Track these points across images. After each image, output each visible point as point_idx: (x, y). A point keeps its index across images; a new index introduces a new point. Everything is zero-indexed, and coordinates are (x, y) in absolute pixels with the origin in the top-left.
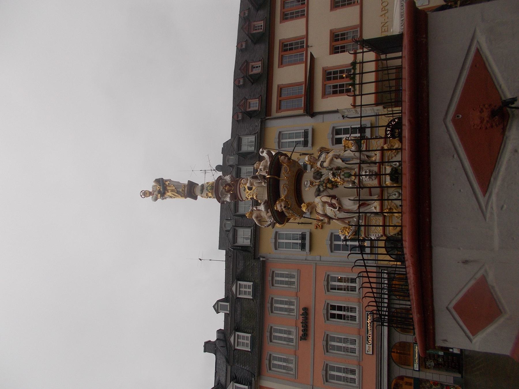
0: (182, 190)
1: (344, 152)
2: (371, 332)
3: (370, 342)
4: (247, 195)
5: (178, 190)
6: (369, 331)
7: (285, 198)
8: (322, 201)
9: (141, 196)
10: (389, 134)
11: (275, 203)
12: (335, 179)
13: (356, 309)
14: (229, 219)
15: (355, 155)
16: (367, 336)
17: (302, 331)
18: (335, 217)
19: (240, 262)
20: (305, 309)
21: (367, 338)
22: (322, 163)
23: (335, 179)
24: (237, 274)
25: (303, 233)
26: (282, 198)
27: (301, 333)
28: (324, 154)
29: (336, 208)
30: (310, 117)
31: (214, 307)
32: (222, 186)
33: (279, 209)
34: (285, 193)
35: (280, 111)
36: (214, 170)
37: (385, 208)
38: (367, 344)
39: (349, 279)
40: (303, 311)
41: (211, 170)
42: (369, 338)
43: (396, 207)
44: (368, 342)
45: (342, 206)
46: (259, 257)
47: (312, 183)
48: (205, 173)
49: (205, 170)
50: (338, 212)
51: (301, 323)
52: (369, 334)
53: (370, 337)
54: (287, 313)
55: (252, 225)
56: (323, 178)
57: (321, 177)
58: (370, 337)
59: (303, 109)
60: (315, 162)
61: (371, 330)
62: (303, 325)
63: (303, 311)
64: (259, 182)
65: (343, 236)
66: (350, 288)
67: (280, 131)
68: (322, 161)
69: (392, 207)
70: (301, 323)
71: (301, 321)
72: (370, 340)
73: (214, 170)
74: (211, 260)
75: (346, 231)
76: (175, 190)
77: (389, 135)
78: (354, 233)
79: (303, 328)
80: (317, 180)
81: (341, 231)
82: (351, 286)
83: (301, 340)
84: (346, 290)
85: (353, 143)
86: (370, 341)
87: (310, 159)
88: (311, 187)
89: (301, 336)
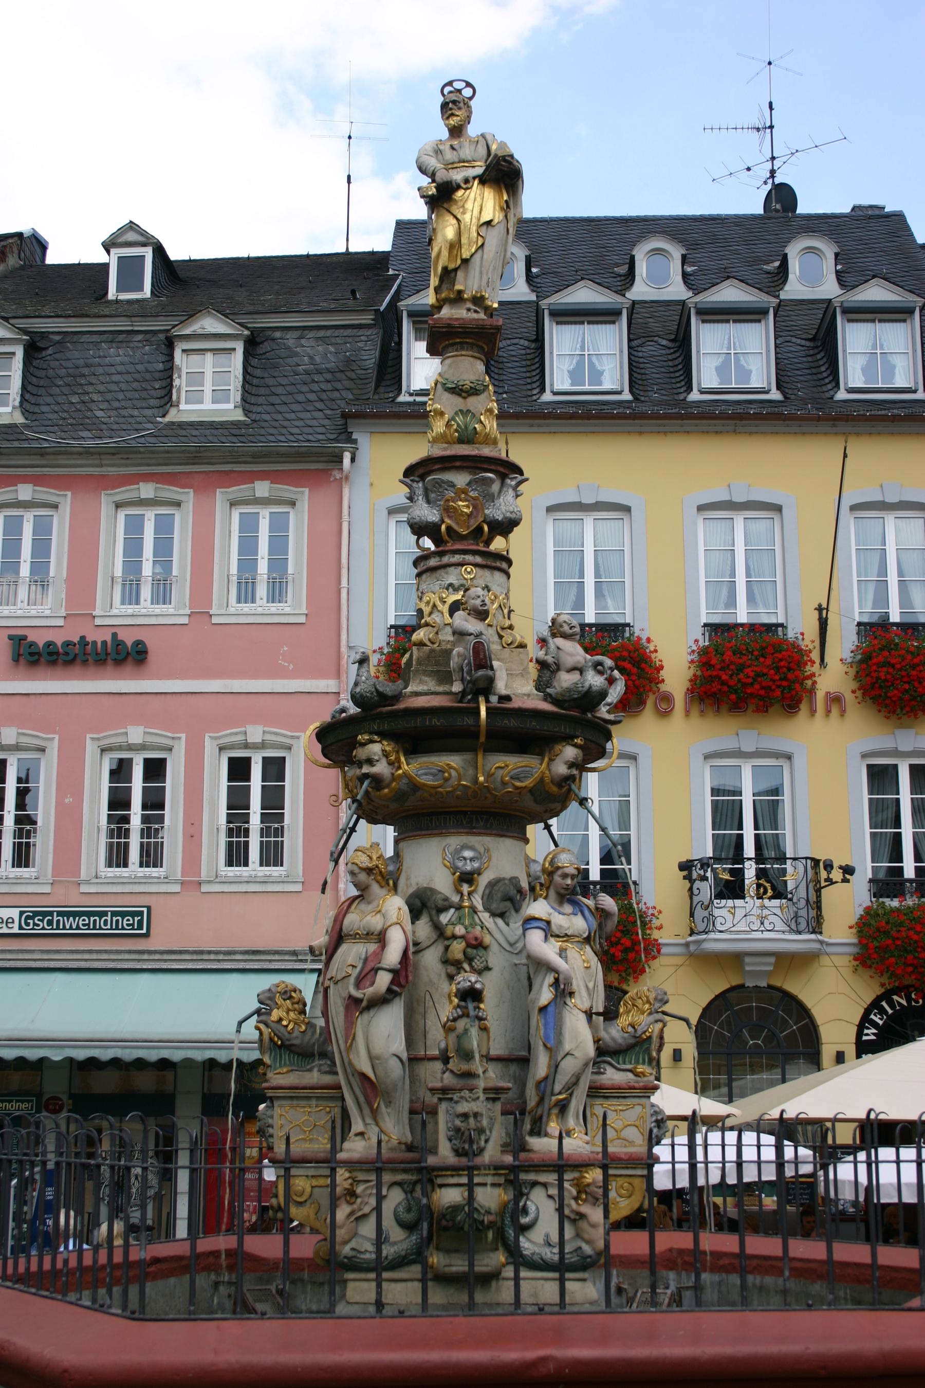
0: (460, 292)
1: (585, 1012)
2: (68, 927)
3: (28, 924)
4: (435, 599)
6: (71, 919)
7: (405, 774)
8: (387, 929)
9: (450, 83)
10: (909, 999)
11: (383, 735)
13: (155, 866)
14: (534, 270)
15: (567, 1054)
16: (51, 914)
17: (49, 644)
18: (330, 979)
19: (332, 349)
20: (139, 653)
21: (44, 914)
24: (278, 334)
27: (40, 639)
28: (586, 926)
31: (132, 226)
32: (469, 484)
36: (773, 173)
37: (355, 1174)
38: (21, 913)
39: (276, 836)
40: (129, 643)
41: (773, 158)
42: (42, 921)
43: (360, 1214)
44: (28, 918)
46: (354, 437)
47: (468, 878)
48: (758, 129)
49: (771, 127)
51: (83, 638)
52: (58, 921)
53: (50, 923)
54: (120, 574)
56: (491, 920)
57: (493, 915)
58: (50, 923)
60: (552, 888)
61: (74, 927)
62: (75, 645)
63: (129, 643)
66: (238, 843)
68: (548, 923)
69: (359, 1200)
70: (83, 638)
71: (89, 639)
72: (38, 925)
73: (773, 173)
74: (349, 181)
75: (288, 1011)
76: (459, 262)
77: (904, 1002)
79: (59, 644)
80: (482, 899)
81: (286, 992)
82: (246, 844)
83: (11, 638)
84: (231, 825)
85: (636, 1030)
86: (31, 927)
87: (559, 872)
88: (454, 874)
89: (29, 639)
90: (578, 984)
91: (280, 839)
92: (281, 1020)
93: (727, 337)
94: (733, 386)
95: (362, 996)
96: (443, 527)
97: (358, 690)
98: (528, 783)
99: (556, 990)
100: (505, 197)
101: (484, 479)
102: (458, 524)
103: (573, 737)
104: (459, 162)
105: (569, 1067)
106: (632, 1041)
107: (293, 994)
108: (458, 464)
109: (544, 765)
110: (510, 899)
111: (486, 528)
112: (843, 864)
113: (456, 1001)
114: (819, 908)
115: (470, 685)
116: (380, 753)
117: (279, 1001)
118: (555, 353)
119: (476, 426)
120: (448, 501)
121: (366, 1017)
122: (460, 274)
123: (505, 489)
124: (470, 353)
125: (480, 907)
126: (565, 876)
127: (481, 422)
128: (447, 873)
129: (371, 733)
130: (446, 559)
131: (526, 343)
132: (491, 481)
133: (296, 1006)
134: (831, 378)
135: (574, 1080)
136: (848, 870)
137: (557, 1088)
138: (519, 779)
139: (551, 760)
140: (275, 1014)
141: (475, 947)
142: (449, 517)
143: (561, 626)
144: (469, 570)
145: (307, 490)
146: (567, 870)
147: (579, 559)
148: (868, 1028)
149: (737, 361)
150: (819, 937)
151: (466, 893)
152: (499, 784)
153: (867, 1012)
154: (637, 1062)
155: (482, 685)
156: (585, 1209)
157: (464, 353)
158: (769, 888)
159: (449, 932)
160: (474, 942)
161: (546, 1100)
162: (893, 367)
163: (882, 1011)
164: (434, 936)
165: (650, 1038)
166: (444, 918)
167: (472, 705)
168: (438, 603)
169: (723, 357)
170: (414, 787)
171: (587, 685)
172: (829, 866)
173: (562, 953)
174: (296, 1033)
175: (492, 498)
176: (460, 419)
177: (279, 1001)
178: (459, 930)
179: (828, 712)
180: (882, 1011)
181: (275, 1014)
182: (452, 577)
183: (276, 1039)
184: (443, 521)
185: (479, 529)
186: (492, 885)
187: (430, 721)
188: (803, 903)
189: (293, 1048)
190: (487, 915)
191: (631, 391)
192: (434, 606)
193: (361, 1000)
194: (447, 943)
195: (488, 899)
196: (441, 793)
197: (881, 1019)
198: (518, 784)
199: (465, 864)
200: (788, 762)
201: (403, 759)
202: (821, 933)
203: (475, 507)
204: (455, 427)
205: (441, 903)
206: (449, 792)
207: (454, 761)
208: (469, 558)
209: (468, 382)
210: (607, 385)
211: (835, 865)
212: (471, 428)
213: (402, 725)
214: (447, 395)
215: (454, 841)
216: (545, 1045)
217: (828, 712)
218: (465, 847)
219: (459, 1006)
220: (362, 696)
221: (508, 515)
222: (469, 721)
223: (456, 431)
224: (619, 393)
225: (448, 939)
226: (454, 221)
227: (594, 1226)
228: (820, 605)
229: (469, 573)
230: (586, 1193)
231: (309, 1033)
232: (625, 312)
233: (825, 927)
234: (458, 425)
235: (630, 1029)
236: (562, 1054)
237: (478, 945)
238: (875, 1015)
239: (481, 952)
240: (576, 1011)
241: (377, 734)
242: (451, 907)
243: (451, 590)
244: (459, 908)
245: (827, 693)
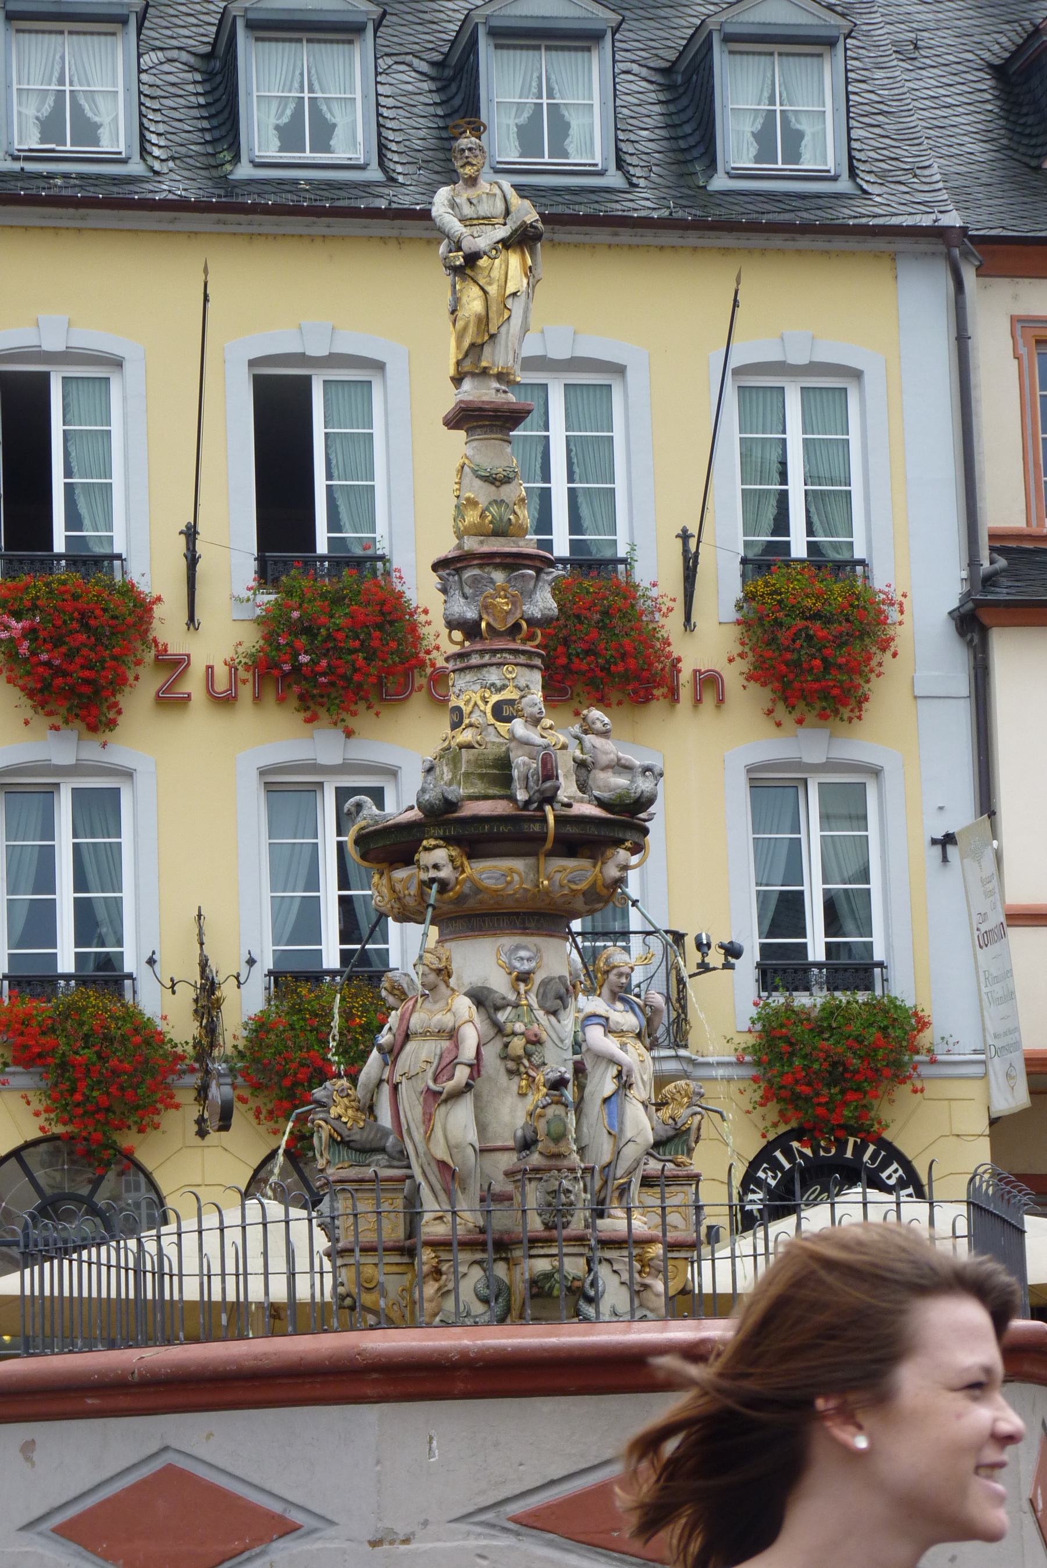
1: (643, 1103)
5: (485, 347)
11: (449, 841)
12: (541, 1088)
23: (541, 1088)
25: (117, 563)
26: (468, 870)
29: (435, 1080)
30: (955, 604)
33: (426, 858)
34: (489, 878)
35: (1023, 351)
37: (440, 1254)
45: (446, 1101)
47: (524, 977)
50: (421, 1087)
55: (157, 166)
59: (1028, 531)
64: (527, 778)
65: (327, 1097)
67: (867, 378)
68: (607, 1019)
69: (444, 1277)
75: (347, 1108)
76: (486, 338)
77: (808, 1151)
78: (339, 1139)
81: (343, 1090)
85: (676, 1124)
87: (615, 971)
88: (510, 974)
90: (636, 1078)
92: (340, 1116)
93: (535, 75)
94: (546, 160)
95: (440, 1089)
97: (427, 797)
98: (583, 886)
99: (619, 1081)
100: (529, 262)
101: (523, 576)
102: (495, 620)
104: (478, 219)
105: (630, 1153)
106: (671, 1133)
109: (598, 868)
110: (560, 998)
111: (524, 625)
112: (726, 942)
113: (544, 1090)
114: (684, 1008)
115: (537, 795)
117: (337, 1099)
119: (511, 517)
120: (487, 597)
121: (443, 1109)
122: (487, 350)
123: (540, 584)
124: (499, 436)
126: (620, 975)
127: (515, 513)
128: (502, 973)
129: (436, 838)
131: (192, 60)
133: (353, 1103)
134: (701, 149)
135: (635, 1165)
136: (733, 951)
137: (620, 1172)
138: (574, 882)
139: (603, 863)
140: (334, 1112)
141: (534, 1043)
142: (488, 613)
143: (594, 723)
146: (622, 970)
148: (754, 1192)
150: (682, 1052)
151: (522, 991)
152: (557, 887)
153: (754, 1165)
154: (677, 1153)
155: (548, 794)
156: (648, 1281)
159: (508, 1028)
160: (534, 1039)
161: (610, 1183)
163: (776, 1165)
164: (492, 1032)
165: (689, 1129)
166: (502, 1016)
167: (538, 813)
168: (480, 703)
170: (477, 890)
171: (639, 790)
173: (623, 1046)
174: (355, 1129)
175: (531, 594)
176: (494, 509)
177: (337, 1099)
178: (519, 1027)
179: (698, 701)
181: (334, 1112)
182: (493, 676)
183: (336, 1135)
184: (481, 619)
185: (516, 628)
186: (545, 983)
187: (498, 829)
189: (352, 1144)
191: (381, 164)
192: (476, 704)
193: (441, 1093)
194: (506, 1039)
195: (542, 997)
197: (774, 1178)
198: (574, 887)
199: (523, 964)
202: (686, 1046)
203: (514, 604)
204: (490, 518)
205: (499, 1002)
207: (518, 864)
209: (500, 470)
210: (340, 154)
212: (505, 519)
213: (471, 831)
214: (478, 483)
215: (508, 942)
216: (610, 1133)
217: (698, 701)
218: (518, 948)
219: (547, 1095)
220: (430, 803)
221: (546, 612)
222: (536, 828)
223: (491, 522)
224: (362, 167)
225: (508, 1036)
226: (481, 293)
227: (658, 1295)
228: (685, 530)
229: (511, 673)
230: (649, 1265)
231: (368, 1129)
233: (691, 1037)
234: (493, 516)
235: (671, 1121)
236: (624, 1141)
237: (537, 1042)
238: (764, 1171)
239: (539, 1048)
240: (635, 1101)
241: (441, 839)
242: (508, 1005)
244: (516, 1006)
245: (695, 671)
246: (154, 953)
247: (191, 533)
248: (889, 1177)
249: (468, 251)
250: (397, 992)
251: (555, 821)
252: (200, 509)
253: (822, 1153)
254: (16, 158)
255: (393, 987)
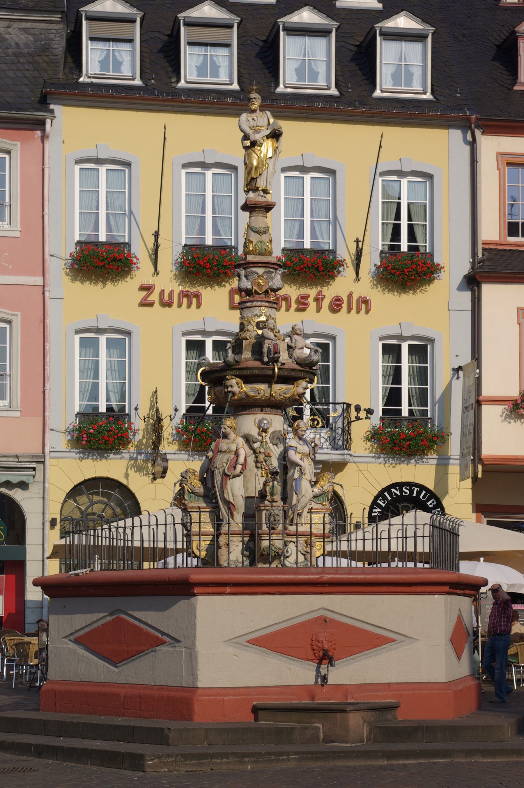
10: (401, 491)
11: (237, 376)
22: (295, 449)
30: (466, 272)
32: (264, 273)
35: (501, 167)
56: (273, 446)
68: (296, 448)
77: (398, 493)
78: (191, 491)
87: (300, 429)
91: (4, 382)
93: (303, 47)
95: (230, 474)
96: (253, 291)
98: (288, 395)
103: (305, 378)
106: (322, 493)
107: (196, 473)
108: (260, 265)
112: (367, 408)
116: (235, 383)
118: (188, 53)
125: (269, 442)
129: (232, 375)
130: (254, 304)
132: (273, 272)
135: (305, 505)
136: (370, 412)
137: (299, 508)
141: (268, 457)
144: (263, 309)
145: (19, 143)
147: (202, 200)
148: (376, 508)
149: (310, 64)
151: (264, 436)
152: (278, 396)
153: (376, 498)
157: (260, 215)
158: (320, 422)
159: (258, 451)
160: (268, 455)
162: (412, 75)
163: (384, 498)
165: (328, 492)
166: (256, 445)
169: (299, 63)
172: (358, 408)
175: (272, 278)
178: (262, 450)
180: (384, 498)
183: (190, 490)
186: (273, 433)
188: (340, 431)
189: (196, 494)
190: (271, 444)
193: (230, 476)
195: (272, 439)
196: (257, 399)
197: (384, 503)
198: (285, 396)
200: (333, 340)
201: (243, 386)
203: (266, 282)
205: (255, 440)
206: (259, 398)
207: (263, 387)
208: (263, 303)
211: (362, 408)
213: (244, 372)
228: (357, 239)
229: (263, 310)
232: (236, 25)
233: (352, 446)
235: (321, 488)
238: (380, 500)
241: (234, 376)
243: (256, 316)
246: (137, 405)
247: (156, 235)
248: (431, 504)
249: (252, 140)
250: (216, 434)
251: (278, 370)
252: (160, 225)
253: (404, 494)
254: (89, 77)
255: (215, 432)
